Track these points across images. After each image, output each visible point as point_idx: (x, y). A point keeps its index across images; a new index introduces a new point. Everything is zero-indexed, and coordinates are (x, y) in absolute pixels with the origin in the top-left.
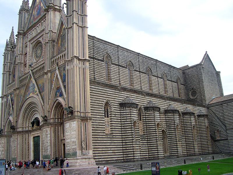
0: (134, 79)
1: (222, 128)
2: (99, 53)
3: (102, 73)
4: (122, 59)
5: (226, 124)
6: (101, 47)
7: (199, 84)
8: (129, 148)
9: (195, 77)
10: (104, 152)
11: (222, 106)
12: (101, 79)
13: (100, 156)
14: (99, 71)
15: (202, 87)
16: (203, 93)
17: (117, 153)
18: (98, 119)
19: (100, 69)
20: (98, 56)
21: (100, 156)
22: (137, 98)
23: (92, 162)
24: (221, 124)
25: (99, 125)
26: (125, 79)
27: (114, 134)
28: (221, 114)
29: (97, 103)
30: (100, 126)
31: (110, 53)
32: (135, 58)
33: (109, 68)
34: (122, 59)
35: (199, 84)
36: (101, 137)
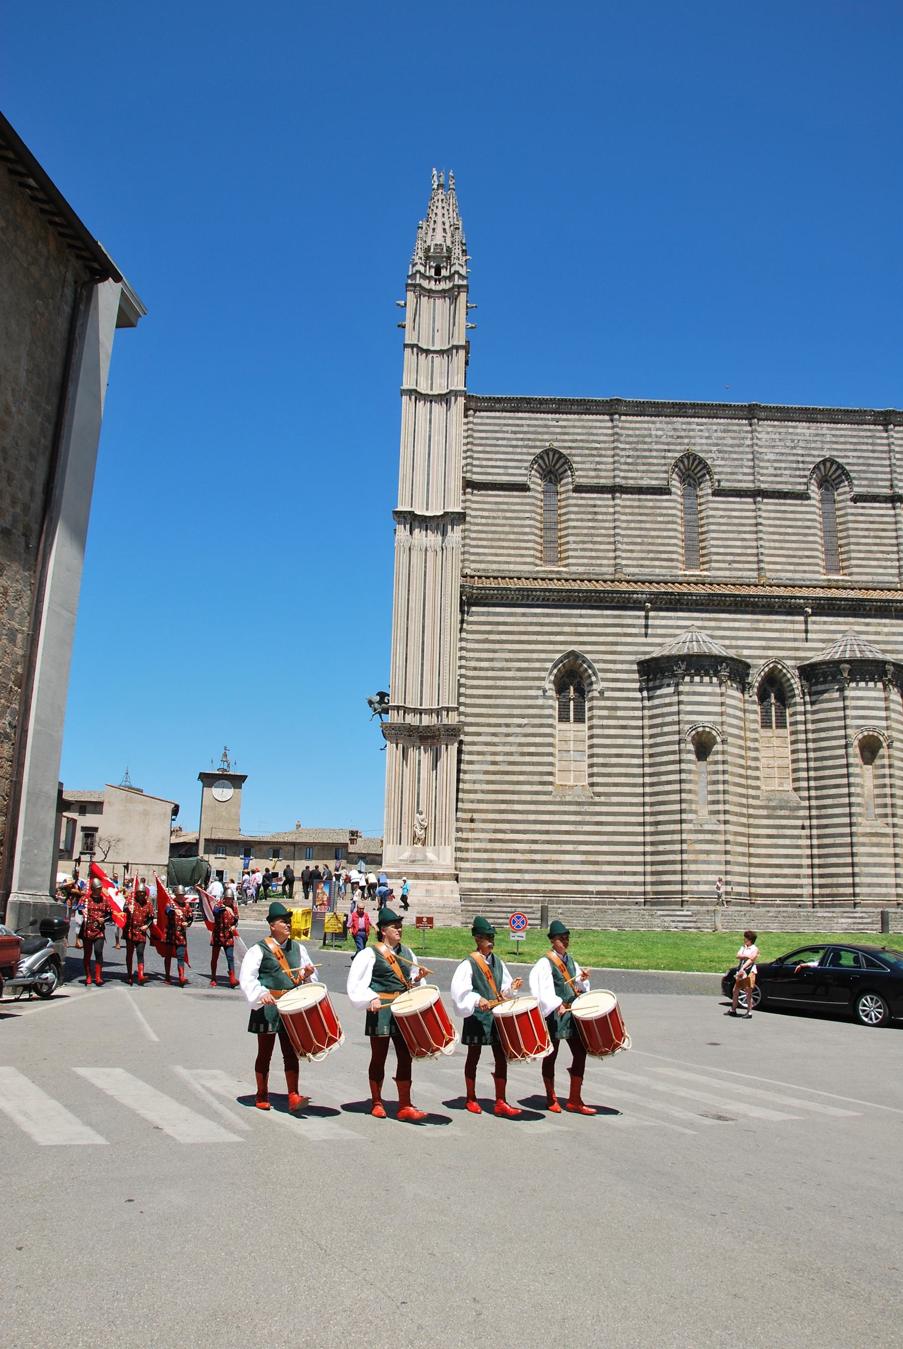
0: (853, 540)
2: (645, 461)
3: (659, 541)
4: (775, 461)
6: (653, 433)
8: (668, 847)
12: (654, 567)
13: (519, 871)
14: (643, 533)
17: (609, 863)
18: (519, 730)
19: (648, 526)
20: (639, 475)
21: (519, 871)
22: (757, 630)
25: (523, 754)
26: (794, 545)
29: (519, 669)
30: (527, 759)
31: (705, 448)
32: (866, 440)
33: (701, 512)
34: (775, 461)
36: (528, 798)
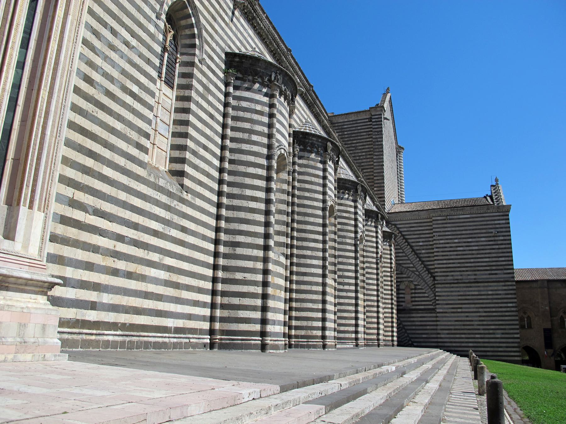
1: (423, 279)
5: (436, 270)
7: (368, 156)
9: (360, 138)
10: (121, 265)
11: (431, 222)
13: (96, 287)
15: (379, 166)
16: (378, 180)
17: (189, 288)
21: (96, 287)
23: (23, 326)
24: (420, 267)
25: (125, 89)
27: (187, 182)
28: (423, 242)
30: (128, 100)
35: (368, 156)
36: (121, 161)
